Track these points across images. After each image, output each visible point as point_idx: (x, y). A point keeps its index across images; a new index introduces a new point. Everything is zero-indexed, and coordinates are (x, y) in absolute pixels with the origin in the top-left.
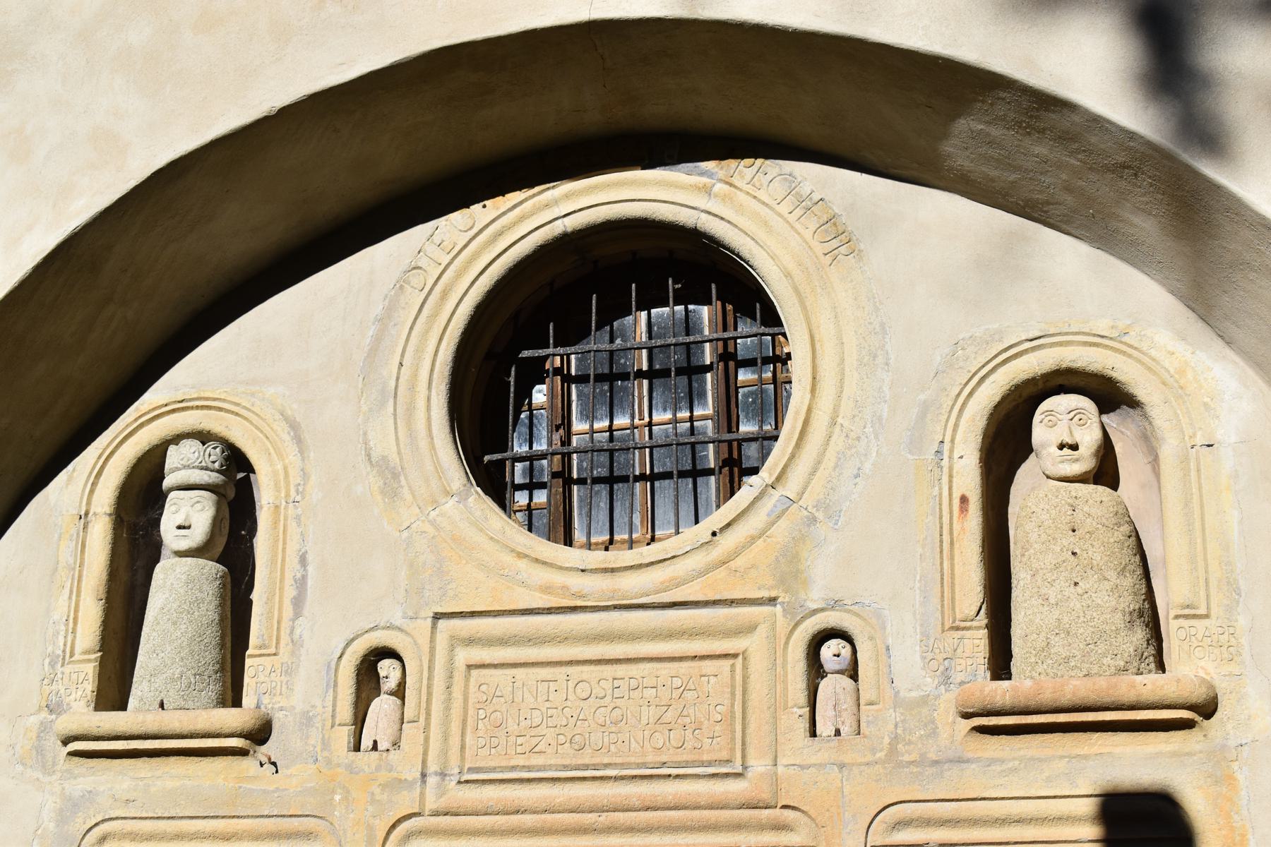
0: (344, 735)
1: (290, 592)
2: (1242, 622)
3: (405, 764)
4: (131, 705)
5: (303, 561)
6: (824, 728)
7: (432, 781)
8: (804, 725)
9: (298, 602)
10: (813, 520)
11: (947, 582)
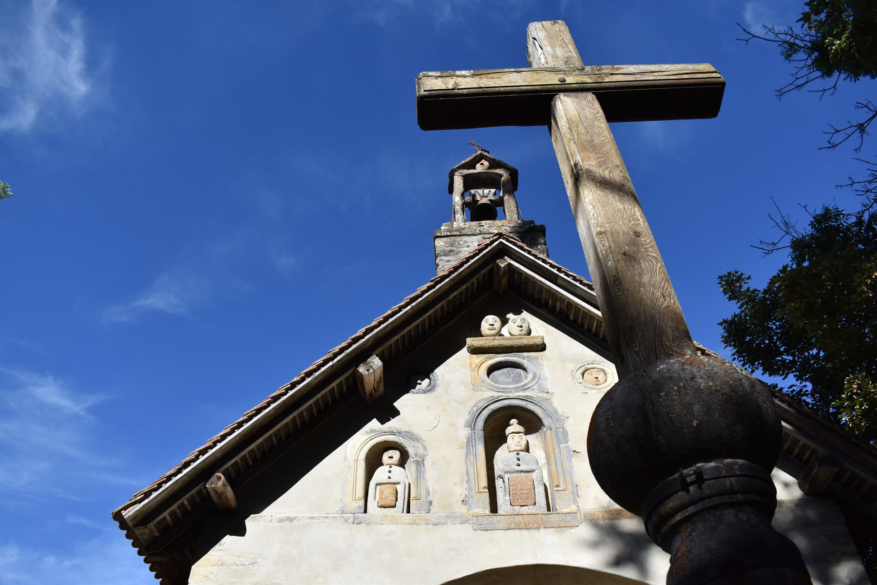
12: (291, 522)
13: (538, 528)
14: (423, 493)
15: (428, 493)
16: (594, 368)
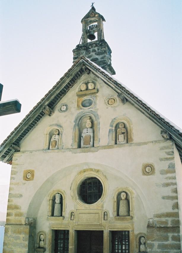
0: (70, 219)
1: (66, 207)
2: (135, 212)
3: (74, 221)
4: (54, 215)
5: (66, 204)
6: (105, 219)
7: (76, 223)
8: (103, 219)
9: (66, 208)
10: (104, 203)
11: (114, 208)
12: (31, 152)
13: (87, 152)
14: (62, 143)
15: (63, 143)
16: (111, 99)
